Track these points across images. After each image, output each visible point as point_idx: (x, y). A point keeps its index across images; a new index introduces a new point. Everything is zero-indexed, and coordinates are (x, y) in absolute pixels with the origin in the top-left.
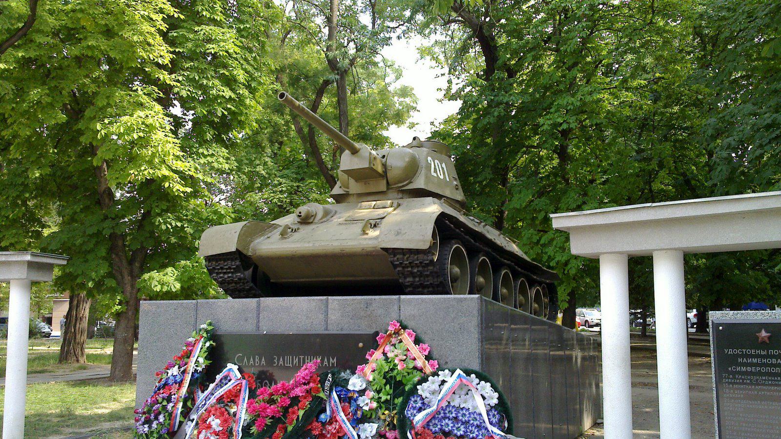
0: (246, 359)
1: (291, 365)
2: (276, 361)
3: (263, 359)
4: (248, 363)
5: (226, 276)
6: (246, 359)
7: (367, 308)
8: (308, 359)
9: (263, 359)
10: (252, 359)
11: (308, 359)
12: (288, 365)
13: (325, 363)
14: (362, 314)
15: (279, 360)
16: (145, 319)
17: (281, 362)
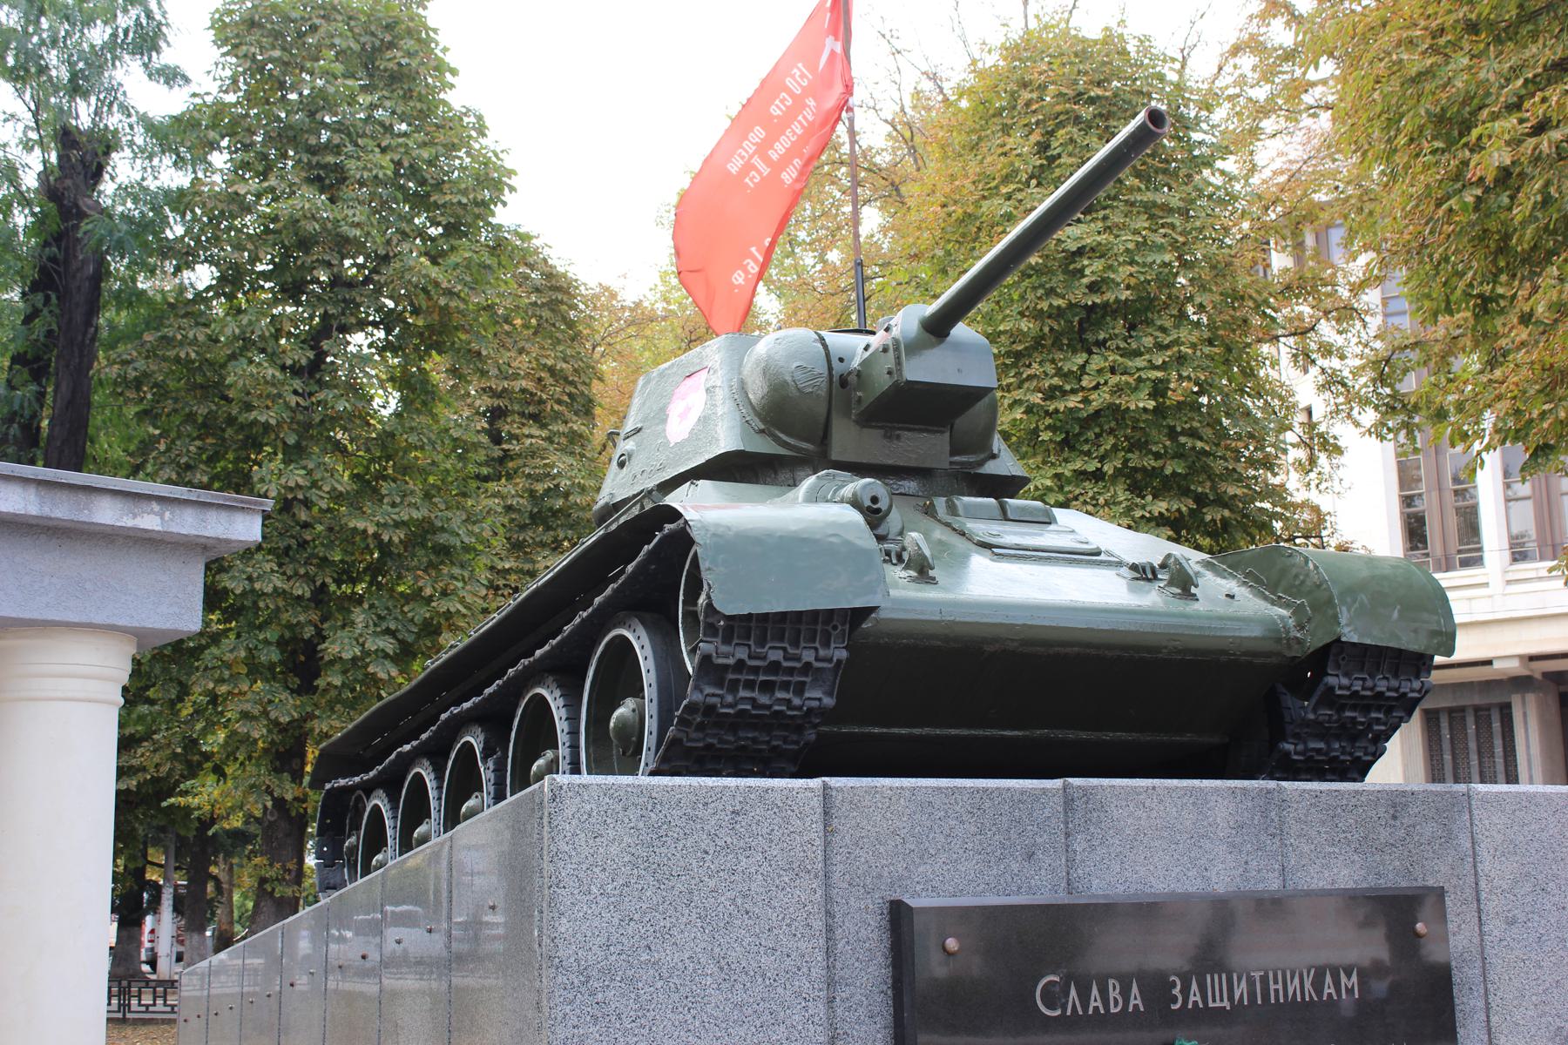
0: (1073, 993)
1: (1226, 1004)
2: (1176, 991)
3: (1135, 989)
4: (1085, 1006)
5: (764, 699)
6: (1073, 993)
7: (1394, 817)
8: (1276, 982)
9: (1135, 989)
10: (1095, 992)
11: (1276, 982)
12: (1218, 1004)
13: (1326, 991)
14: (1384, 835)
15: (1185, 991)
16: (586, 851)
17: (1195, 997)
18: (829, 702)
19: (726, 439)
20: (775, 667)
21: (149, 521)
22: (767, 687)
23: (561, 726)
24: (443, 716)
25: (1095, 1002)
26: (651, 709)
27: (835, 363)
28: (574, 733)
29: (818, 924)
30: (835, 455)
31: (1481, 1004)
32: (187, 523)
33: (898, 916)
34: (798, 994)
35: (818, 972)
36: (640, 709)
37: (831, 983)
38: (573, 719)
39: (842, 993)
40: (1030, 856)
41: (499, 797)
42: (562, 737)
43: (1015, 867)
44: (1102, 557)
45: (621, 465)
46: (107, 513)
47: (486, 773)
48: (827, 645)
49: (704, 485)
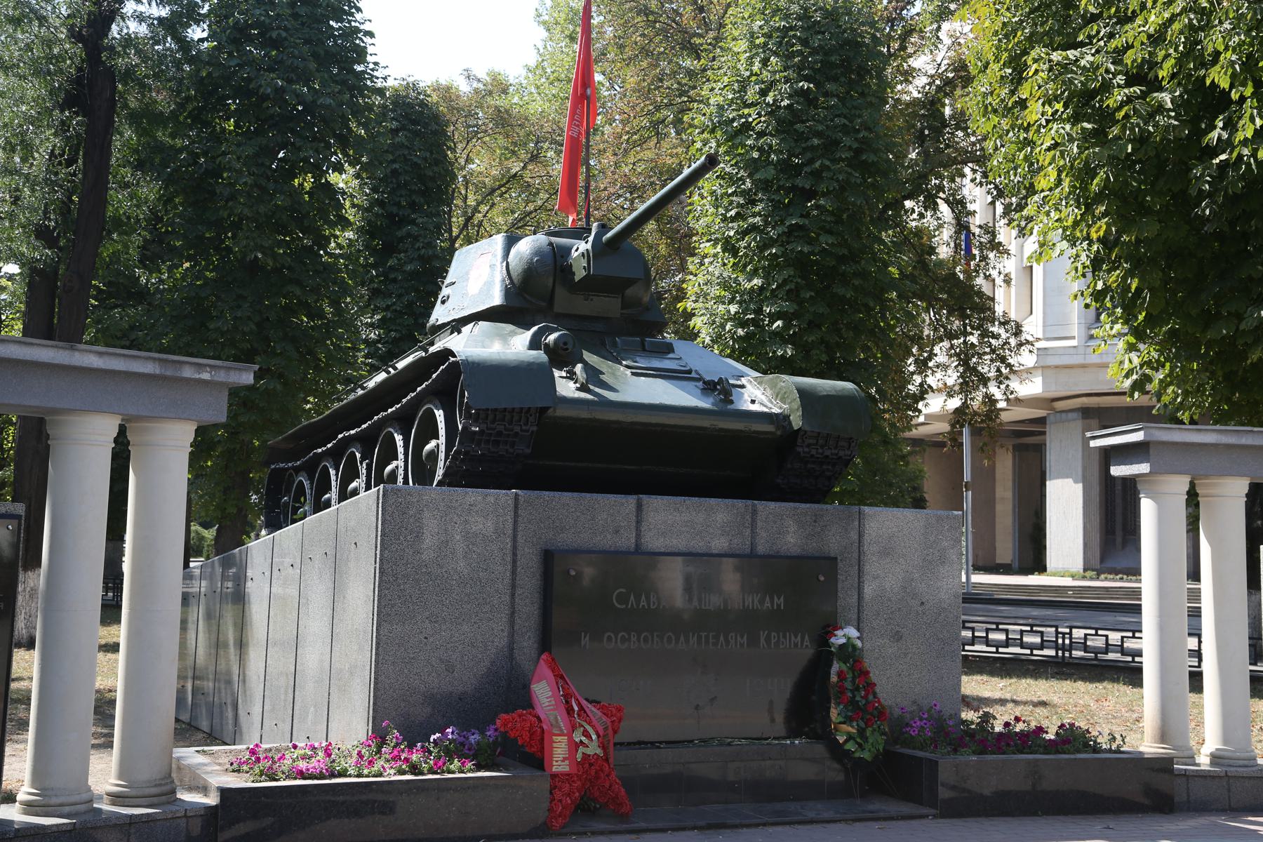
18: (528, 451)
19: (497, 299)
20: (500, 434)
21: (206, 376)
22: (497, 443)
23: (401, 450)
24: (340, 436)
25: (643, 603)
26: (443, 448)
27: (558, 258)
28: (406, 454)
29: (509, 559)
30: (558, 308)
31: (855, 616)
32: (221, 376)
33: (548, 557)
34: (497, 591)
35: (507, 581)
36: (438, 444)
37: (513, 586)
38: (406, 447)
39: (519, 591)
40: (617, 532)
41: (368, 488)
42: (401, 456)
43: (609, 537)
44: (693, 375)
45: (443, 302)
46: (188, 373)
47: (363, 470)
48: (526, 424)
49: (483, 325)
